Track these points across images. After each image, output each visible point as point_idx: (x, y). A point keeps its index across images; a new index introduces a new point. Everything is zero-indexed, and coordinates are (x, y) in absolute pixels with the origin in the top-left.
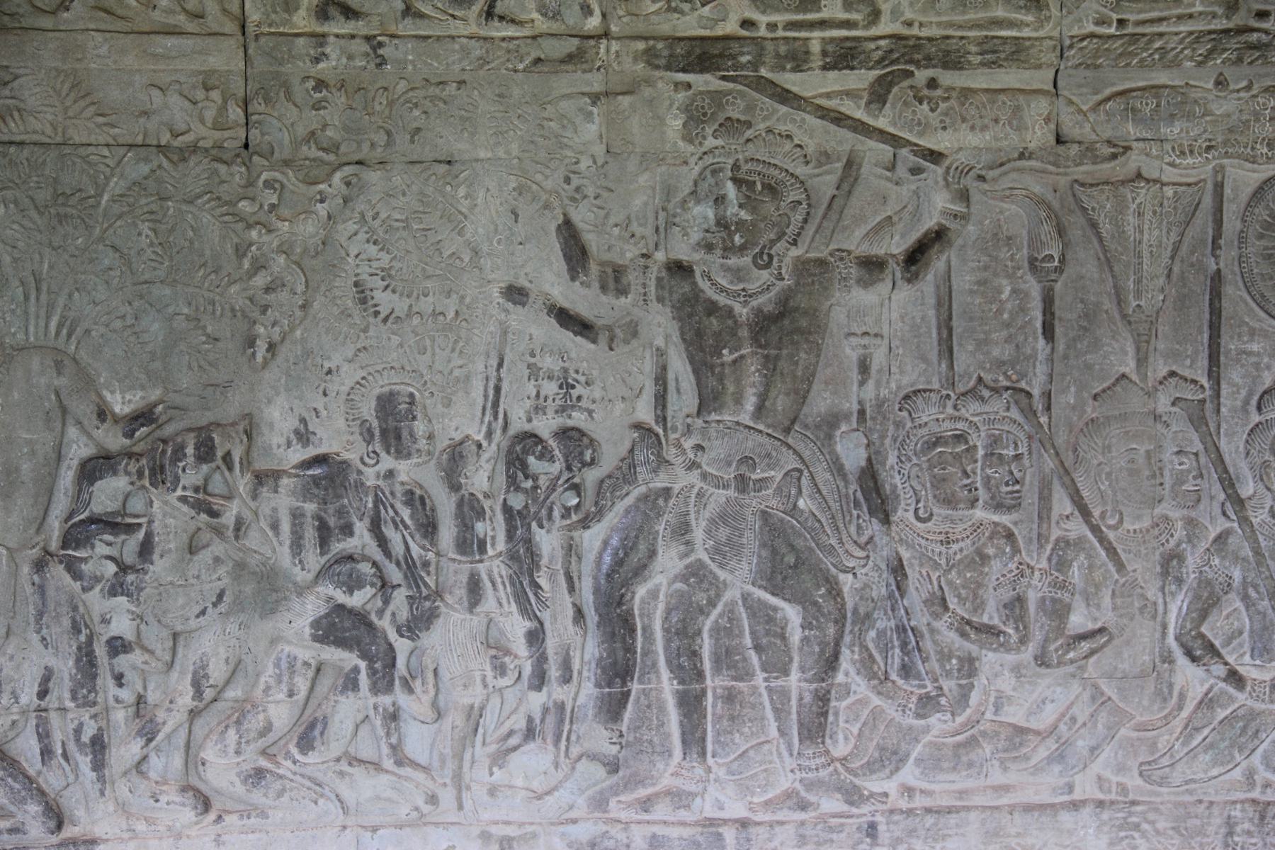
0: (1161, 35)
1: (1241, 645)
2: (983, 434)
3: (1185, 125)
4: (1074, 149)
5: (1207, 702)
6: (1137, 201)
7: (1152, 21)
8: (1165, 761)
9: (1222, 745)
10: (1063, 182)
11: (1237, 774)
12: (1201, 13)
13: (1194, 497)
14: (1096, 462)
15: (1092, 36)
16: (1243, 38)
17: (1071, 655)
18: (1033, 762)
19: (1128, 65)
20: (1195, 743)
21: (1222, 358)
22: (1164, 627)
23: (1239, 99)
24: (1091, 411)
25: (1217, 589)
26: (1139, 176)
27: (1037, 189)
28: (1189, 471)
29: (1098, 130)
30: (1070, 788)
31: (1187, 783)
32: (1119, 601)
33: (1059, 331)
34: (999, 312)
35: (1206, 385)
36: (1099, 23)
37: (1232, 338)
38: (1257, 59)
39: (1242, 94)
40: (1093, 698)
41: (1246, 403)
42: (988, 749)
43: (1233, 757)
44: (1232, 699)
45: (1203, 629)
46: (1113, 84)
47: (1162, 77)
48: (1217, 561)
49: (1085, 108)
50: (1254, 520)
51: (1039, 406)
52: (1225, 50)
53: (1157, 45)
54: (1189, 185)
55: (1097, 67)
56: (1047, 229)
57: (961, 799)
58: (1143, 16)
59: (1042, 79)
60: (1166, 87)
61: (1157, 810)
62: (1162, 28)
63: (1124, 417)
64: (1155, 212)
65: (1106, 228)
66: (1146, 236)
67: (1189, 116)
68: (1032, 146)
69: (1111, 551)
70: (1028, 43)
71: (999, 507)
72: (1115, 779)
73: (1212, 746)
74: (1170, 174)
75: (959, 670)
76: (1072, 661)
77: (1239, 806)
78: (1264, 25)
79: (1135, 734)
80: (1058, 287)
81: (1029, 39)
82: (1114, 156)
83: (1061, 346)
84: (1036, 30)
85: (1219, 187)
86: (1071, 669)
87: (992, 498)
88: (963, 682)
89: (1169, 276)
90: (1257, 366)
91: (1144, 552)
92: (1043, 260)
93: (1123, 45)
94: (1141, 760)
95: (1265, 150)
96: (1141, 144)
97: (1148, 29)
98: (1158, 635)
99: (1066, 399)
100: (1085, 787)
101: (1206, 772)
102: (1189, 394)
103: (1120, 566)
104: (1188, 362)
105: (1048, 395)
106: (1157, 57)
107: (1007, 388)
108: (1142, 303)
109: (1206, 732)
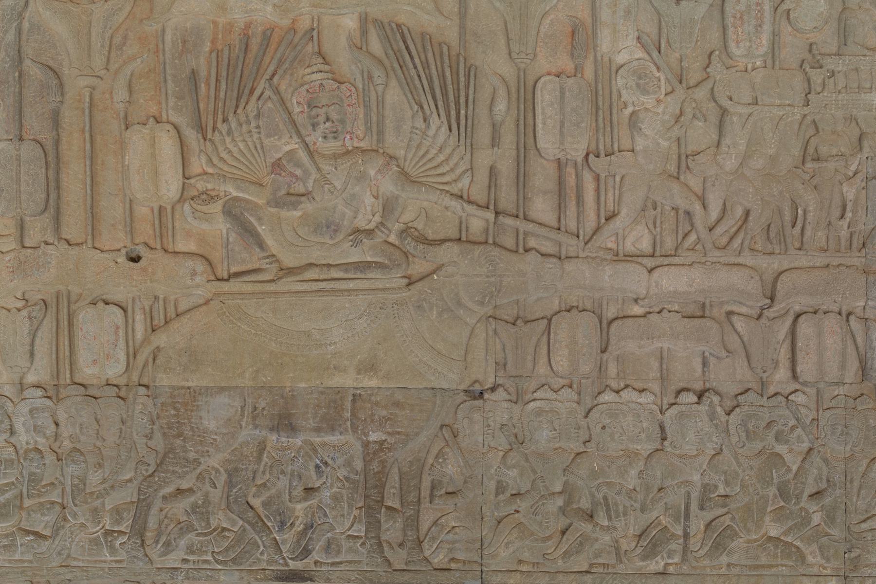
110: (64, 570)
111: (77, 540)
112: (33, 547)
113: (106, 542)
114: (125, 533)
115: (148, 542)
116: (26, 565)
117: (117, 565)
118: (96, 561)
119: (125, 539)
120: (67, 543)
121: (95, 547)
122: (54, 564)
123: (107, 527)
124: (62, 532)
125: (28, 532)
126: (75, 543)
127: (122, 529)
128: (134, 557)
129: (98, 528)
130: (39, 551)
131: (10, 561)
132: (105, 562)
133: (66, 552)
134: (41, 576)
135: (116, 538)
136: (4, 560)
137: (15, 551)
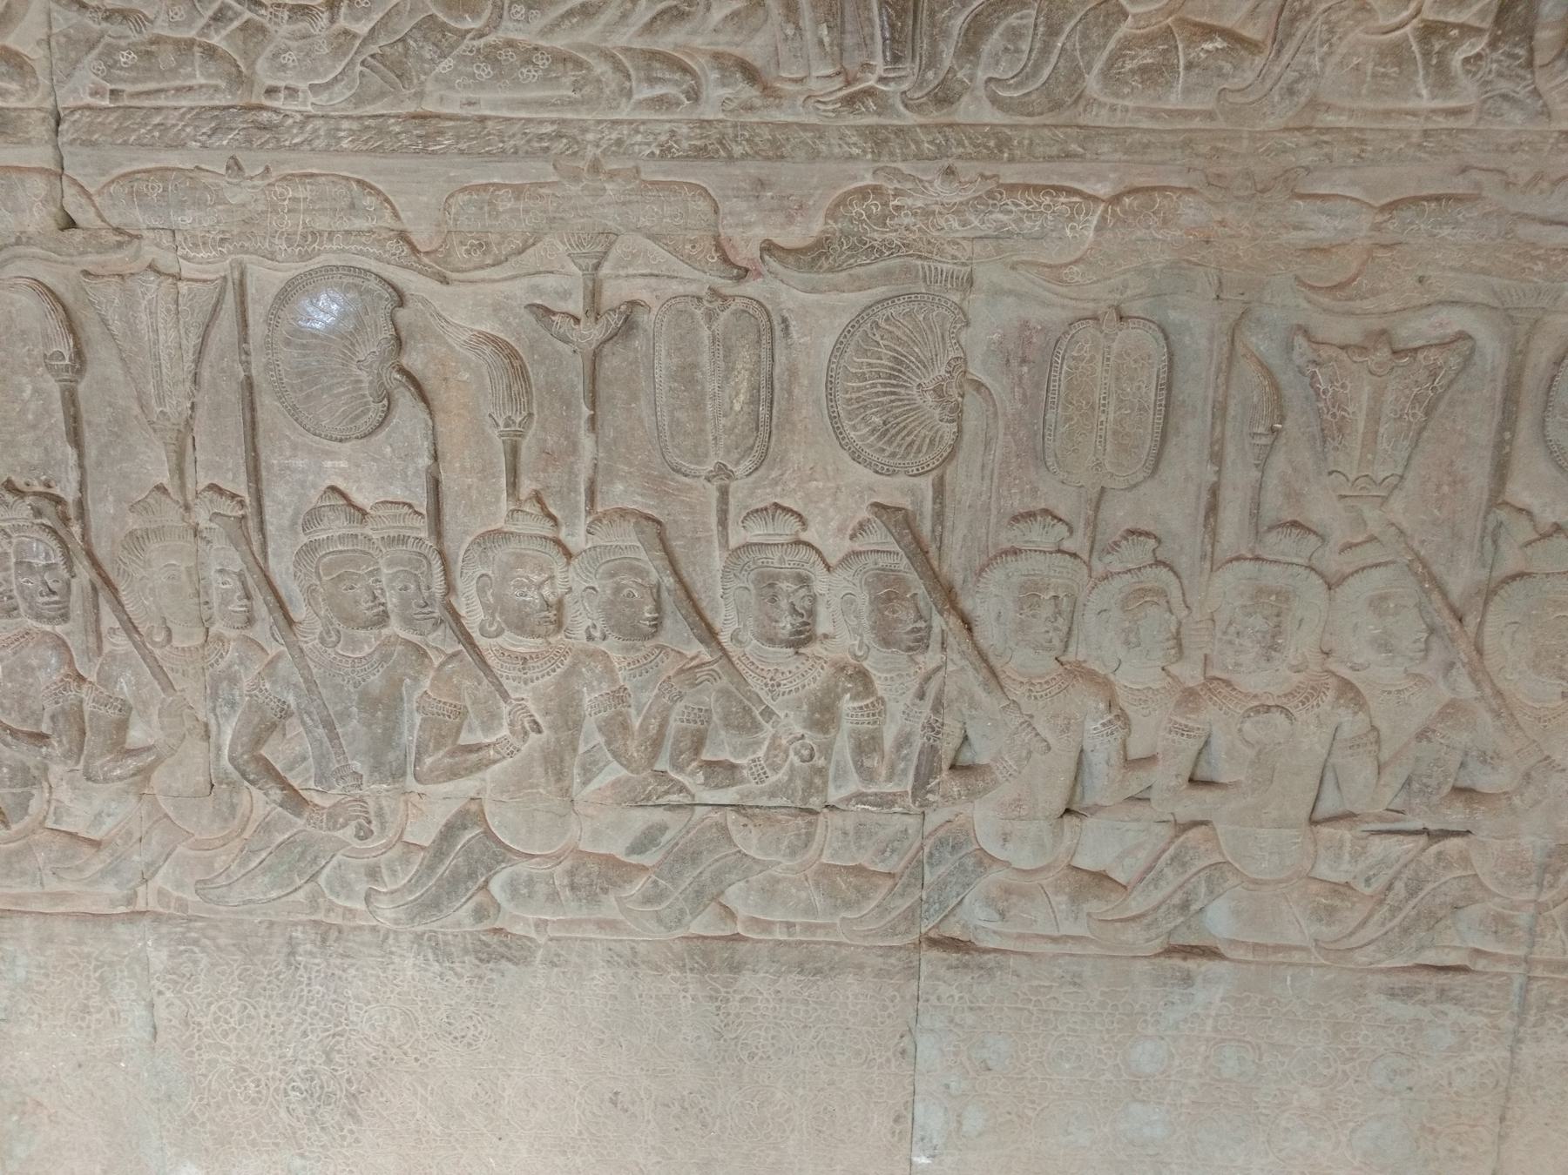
0: (158, 109)
1: (307, 770)
2: (14, 541)
3: (197, 214)
4: (77, 236)
5: (266, 827)
6: (149, 297)
7: (148, 93)
8: (222, 881)
9: (281, 869)
10: (74, 271)
11: (300, 896)
12: (201, 86)
13: (243, 618)
14: (138, 576)
15: (89, 108)
16: (250, 116)
17: (118, 772)
18: (87, 874)
19: (125, 143)
20: (253, 865)
21: (264, 473)
22: (219, 748)
23: (254, 187)
24: (133, 522)
25: (270, 714)
26: (152, 267)
27: (48, 280)
28: (234, 591)
29: (106, 214)
30: (130, 900)
31: (245, 903)
32: (166, 720)
33: (88, 435)
34: (23, 412)
35: (247, 501)
36: (94, 94)
37: (273, 452)
38: (267, 142)
39: (257, 182)
40: (149, 815)
41: (294, 523)
42: (41, 857)
43: (293, 881)
44: (291, 825)
45: (264, 752)
46: (120, 165)
47: (173, 159)
48: (268, 686)
49: (92, 190)
50: (304, 646)
51: (72, 512)
52: (232, 129)
53: (157, 120)
54: (205, 281)
55: (93, 144)
56: (54, 324)
57: (17, 904)
58: (140, 87)
59: (41, 156)
60: (174, 169)
61: (216, 927)
62: (161, 102)
63: (160, 532)
64: (168, 311)
65: (116, 325)
66: (162, 337)
67: (199, 204)
68: (31, 229)
69: (158, 671)
70: (13, 114)
71: (38, 617)
72: (176, 894)
73: (270, 868)
74: (188, 270)
75: (11, 779)
76: (120, 778)
77: (300, 928)
78: (275, 104)
79: (192, 853)
80: (82, 388)
81: (15, 109)
82: (120, 245)
83: (92, 452)
84: (22, 100)
85: (241, 286)
86: (120, 785)
87: (30, 607)
88: (19, 790)
89: (195, 382)
90: (302, 484)
91: (192, 672)
92: (51, 357)
93: (117, 119)
94: (198, 878)
95: (285, 246)
96: (151, 234)
97: (147, 103)
98: (212, 755)
99: (102, 511)
100: (147, 899)
101: (264, 894)
102: (229, 509)
103: (168, 686)
104: (230, 475)
105: (81, 504)
106: (157, 134)
107: (35, 494)
108: (167, 410)
109: (264, 854)
110: (1290, 140)
111: (1342, 49)
112: (1220, 74)
113: (1426, 55)
114: (1479, 31)
115: (1539, 59)
116: (1197, 123)
117: (1452, 123)
118: (1387, 114)
119: (1480, 45)
120: (1315, 61)
121: (1393, 70)
122: (1272, 122)
123: (1429, 14)
124: (1303, 27)
125: (1209, 32)
126: (1336, 59)
127: (1466, 16)
128: (1505, 97)
129: (1405, 14)
130: (1235, 83)
131: (1154, 115)
132: (1414, 114)
133: (1306, 88)
134: (1235, 156)
135: (1454, 45)
136: (1138, 110)
137: (1169, 85)
